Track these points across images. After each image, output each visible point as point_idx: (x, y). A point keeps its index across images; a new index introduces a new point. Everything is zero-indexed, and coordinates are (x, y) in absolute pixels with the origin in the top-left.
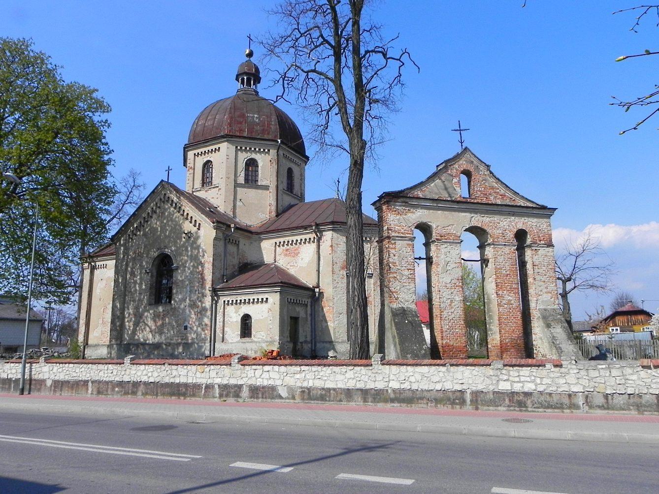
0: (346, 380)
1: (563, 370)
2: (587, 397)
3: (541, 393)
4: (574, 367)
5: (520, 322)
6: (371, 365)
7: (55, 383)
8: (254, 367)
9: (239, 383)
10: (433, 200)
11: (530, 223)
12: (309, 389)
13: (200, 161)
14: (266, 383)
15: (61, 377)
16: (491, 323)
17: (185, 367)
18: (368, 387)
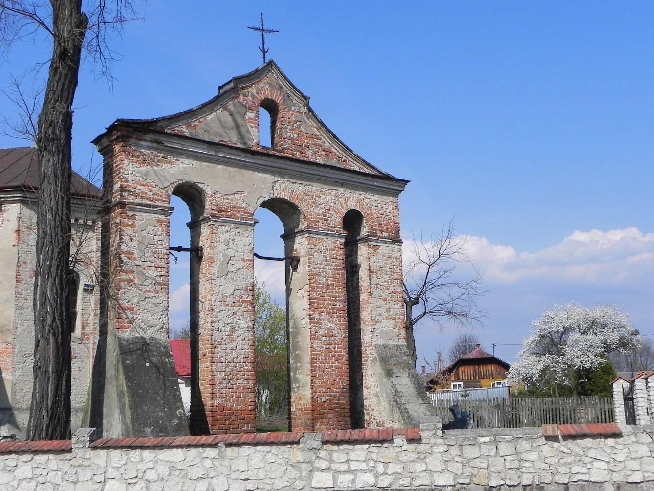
0: (15, 483)
1: (422, 447)
4: (440, 441)
5: (345, 367)
6: (70, 451)
10: (211, 144)
11: (367, 201)
16: (297, 369)
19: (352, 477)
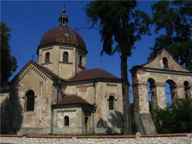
8: (83, 139)
17: (51, 139)
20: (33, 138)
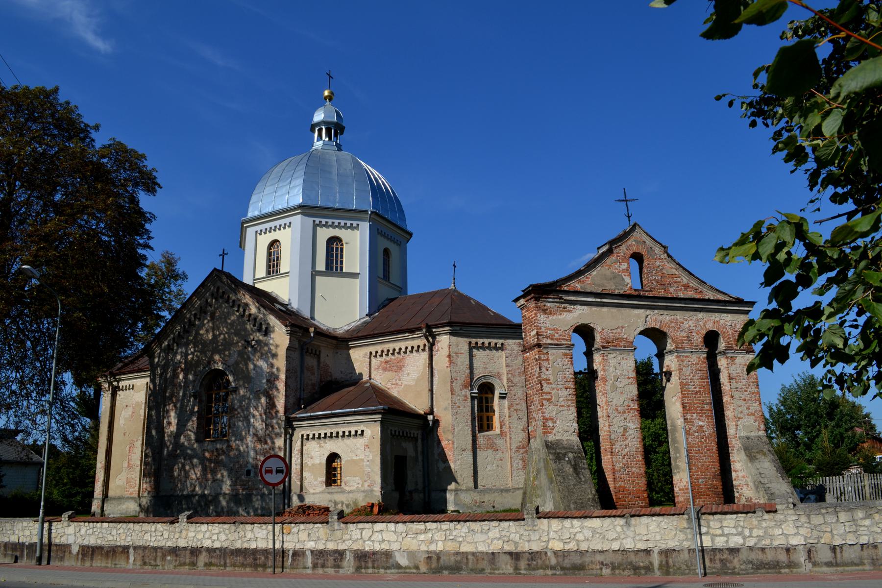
0: (489, 541)
1: (778, 517)
2: (809, 551)
3: (751, 549)
4: (792, 512)
5: (715, 455)
6: (524, 520)
7: (83, 550)
8: (360, 525)
9: (341, 547)
11: (722, 322)
12: (438, 555)
13: (264, 241)
14: (377, 547)
15: (92, 541)
16: (677, 458)
18: (519, 549)
19: (726, 539)
20: (210, 528)
